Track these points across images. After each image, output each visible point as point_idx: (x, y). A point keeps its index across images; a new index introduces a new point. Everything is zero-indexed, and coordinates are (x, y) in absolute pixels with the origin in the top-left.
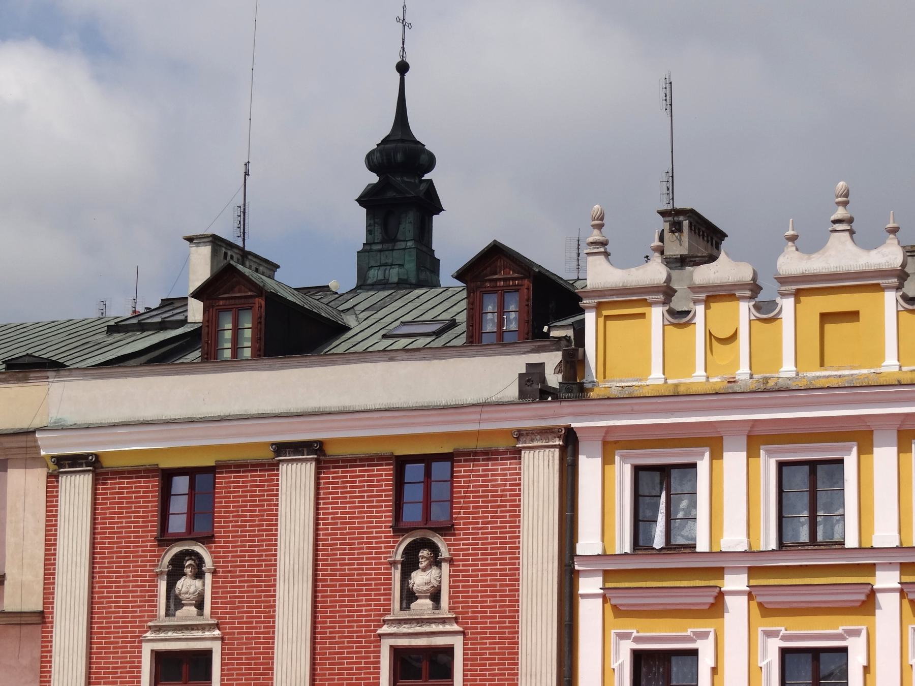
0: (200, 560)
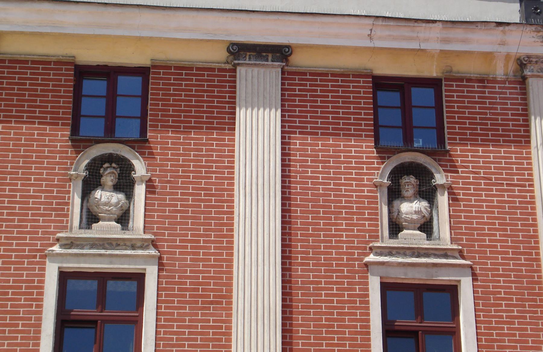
0: (125, 169)
